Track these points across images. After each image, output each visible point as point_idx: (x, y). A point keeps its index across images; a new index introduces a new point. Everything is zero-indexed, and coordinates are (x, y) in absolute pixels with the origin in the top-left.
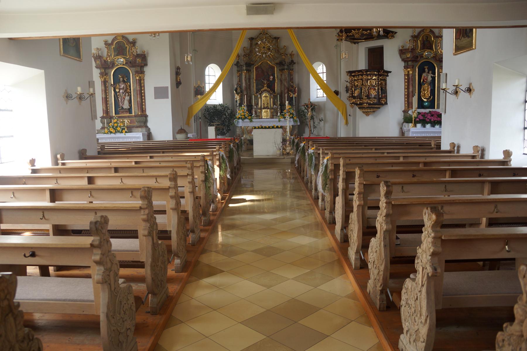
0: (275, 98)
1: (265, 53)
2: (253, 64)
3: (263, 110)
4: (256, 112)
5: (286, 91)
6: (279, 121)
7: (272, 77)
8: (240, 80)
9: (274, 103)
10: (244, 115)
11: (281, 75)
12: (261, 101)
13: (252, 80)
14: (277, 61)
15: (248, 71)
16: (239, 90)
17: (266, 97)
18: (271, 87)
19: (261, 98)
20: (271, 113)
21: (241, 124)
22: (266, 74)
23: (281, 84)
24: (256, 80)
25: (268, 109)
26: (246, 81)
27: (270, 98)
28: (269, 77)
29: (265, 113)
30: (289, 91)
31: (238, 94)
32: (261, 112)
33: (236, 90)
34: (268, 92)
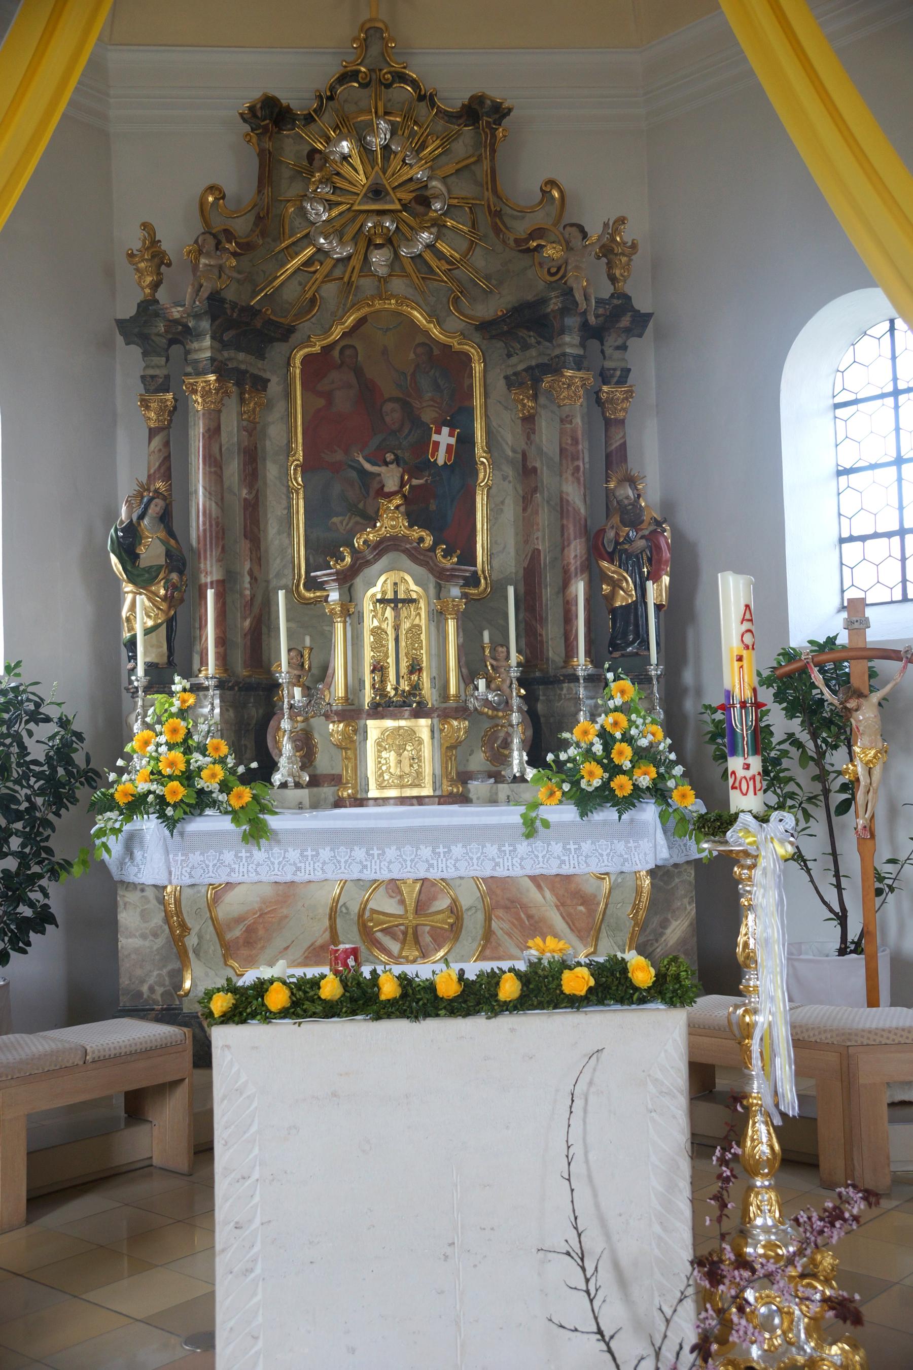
0: (478, 615)
1: (390, 241)
2: (286, 333)
3: (374, 728)
4: (306, 745)
5: (576, 550)
6: (531, 828)
7: (444, 438)
8: (169, 467)
9: (471, 670)
10: (188, 777)
11: (529, 420)
13: (272, 471)
14: (488, 310)
15: (244, 383)
16: (152, 550)
17: (396, 602)
18: (441, 512)
19: (350, 610)
20: (450, 750)
21: (155, 859)
22: (392, 414)
23: (526, 501)
24: (306, 468)
25: (420, 712)
26: (215, 464)
27: (438, 617)
28: (424, 444)
29: (394, 755)
30: (597, 549)
31: (141, 578)
32: (352, 746)
33: (128, 548)
34: (419, 556)
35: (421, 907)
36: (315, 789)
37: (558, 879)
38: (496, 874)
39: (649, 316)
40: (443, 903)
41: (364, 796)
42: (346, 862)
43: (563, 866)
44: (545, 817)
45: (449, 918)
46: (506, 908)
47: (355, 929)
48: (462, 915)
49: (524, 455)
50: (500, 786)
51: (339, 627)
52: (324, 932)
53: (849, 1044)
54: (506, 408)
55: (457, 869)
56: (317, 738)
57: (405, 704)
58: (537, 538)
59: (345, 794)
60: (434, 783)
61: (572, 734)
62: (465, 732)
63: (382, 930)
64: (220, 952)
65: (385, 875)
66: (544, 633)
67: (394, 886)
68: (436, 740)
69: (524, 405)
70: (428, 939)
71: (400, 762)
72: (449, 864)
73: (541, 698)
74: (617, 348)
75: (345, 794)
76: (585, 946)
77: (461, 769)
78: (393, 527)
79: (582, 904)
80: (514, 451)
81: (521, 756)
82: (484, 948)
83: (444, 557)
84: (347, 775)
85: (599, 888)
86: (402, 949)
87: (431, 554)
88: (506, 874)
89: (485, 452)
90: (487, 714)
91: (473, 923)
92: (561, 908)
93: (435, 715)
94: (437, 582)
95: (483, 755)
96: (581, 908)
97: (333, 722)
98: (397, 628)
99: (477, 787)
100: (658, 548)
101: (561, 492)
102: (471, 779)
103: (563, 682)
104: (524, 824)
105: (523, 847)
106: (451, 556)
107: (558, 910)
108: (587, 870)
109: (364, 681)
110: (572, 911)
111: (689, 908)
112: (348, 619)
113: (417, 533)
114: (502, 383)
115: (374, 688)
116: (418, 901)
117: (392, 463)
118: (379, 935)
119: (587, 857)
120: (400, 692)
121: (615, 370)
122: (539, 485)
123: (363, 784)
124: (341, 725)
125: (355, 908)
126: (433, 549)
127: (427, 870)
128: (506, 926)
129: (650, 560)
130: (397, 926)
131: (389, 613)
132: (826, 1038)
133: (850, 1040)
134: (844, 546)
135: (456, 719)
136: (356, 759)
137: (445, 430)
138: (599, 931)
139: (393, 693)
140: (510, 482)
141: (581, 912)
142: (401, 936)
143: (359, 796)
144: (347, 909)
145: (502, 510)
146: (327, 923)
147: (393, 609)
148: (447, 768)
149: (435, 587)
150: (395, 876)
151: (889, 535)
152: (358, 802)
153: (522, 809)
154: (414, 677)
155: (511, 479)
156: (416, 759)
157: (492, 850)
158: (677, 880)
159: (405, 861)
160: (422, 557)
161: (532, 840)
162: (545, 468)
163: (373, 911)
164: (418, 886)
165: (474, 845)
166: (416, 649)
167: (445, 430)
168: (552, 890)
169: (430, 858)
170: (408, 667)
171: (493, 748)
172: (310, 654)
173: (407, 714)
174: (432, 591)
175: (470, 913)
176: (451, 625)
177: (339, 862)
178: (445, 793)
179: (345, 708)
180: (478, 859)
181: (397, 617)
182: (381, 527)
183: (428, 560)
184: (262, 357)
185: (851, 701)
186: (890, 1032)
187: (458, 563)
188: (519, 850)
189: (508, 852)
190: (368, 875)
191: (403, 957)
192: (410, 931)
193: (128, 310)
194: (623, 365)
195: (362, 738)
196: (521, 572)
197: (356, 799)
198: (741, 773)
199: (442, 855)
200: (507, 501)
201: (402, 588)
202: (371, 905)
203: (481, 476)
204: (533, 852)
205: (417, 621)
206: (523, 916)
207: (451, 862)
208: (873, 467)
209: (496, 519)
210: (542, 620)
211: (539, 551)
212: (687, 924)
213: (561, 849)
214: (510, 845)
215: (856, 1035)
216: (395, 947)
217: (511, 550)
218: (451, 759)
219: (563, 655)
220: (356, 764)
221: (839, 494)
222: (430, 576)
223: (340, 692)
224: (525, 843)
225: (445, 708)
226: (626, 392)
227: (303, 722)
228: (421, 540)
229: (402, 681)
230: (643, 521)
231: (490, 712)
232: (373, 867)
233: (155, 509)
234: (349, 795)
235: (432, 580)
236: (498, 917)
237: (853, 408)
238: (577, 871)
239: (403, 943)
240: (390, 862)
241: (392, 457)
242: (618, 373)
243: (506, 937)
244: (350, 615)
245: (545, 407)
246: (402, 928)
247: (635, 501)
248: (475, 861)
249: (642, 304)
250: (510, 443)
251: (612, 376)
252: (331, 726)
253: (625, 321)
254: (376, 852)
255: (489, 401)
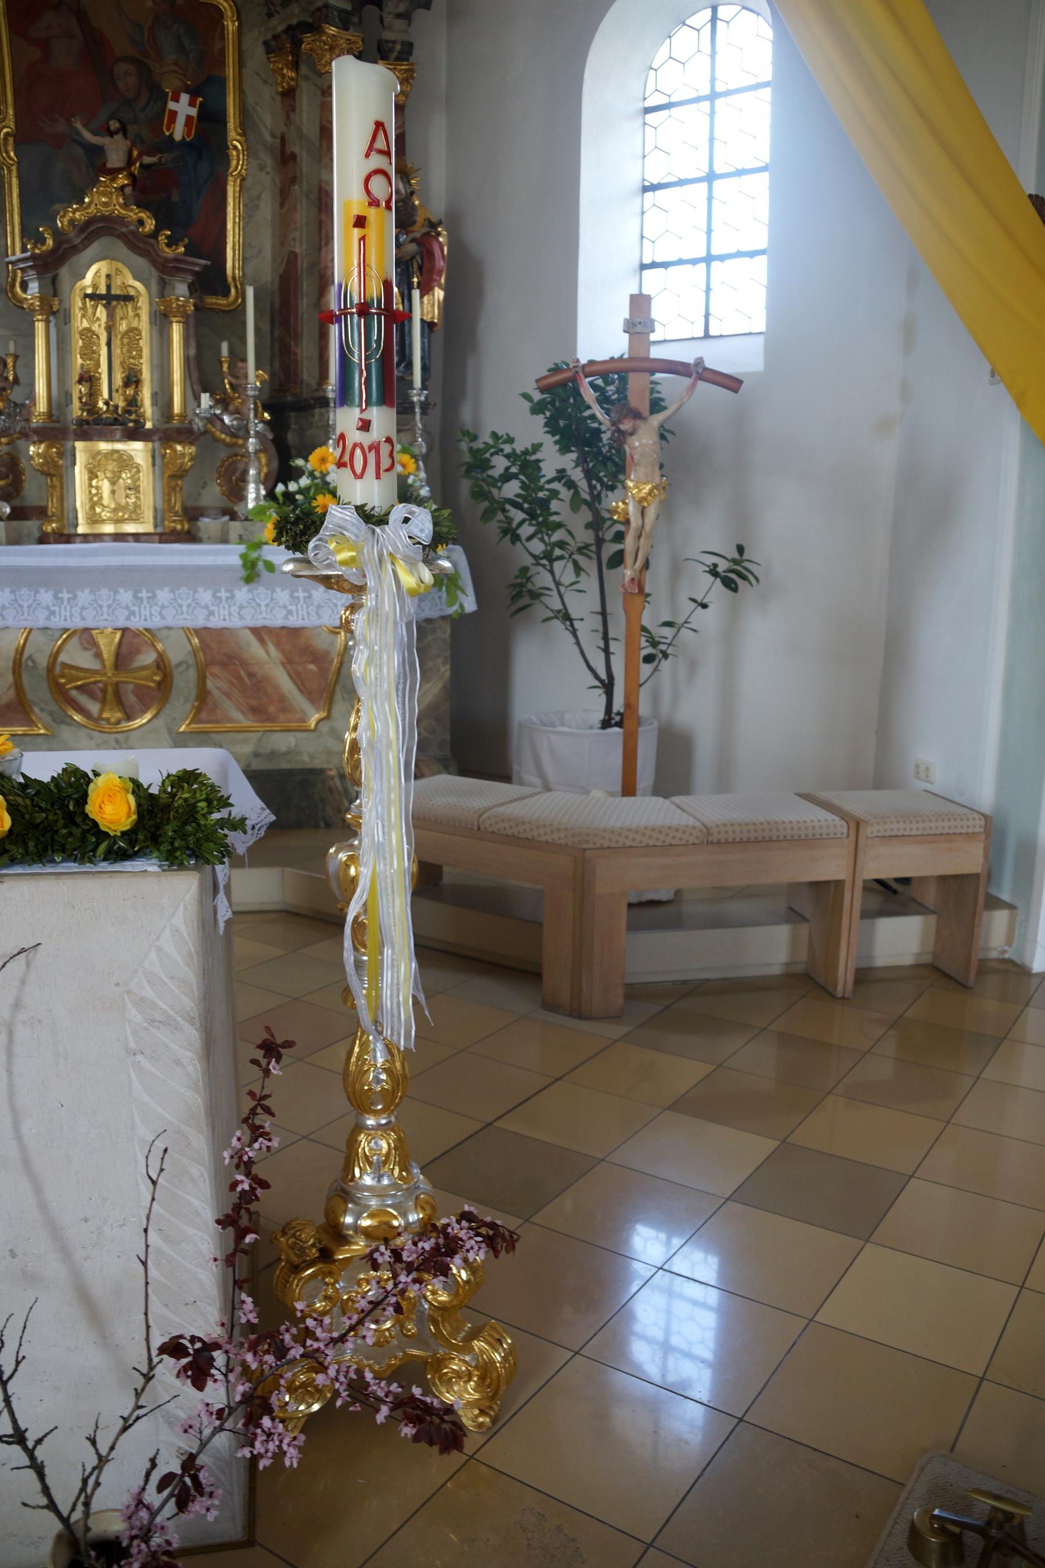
6: (252, 571)
7: (183, 108)
11: (289, 95)
12: (61, 347)
19: (54, 309)
20: (172, 477)
23: (284, 194)
27: (161, 320)
28: (163, 117)
29: (111, 484)
32: (57, 473)
34: (138, 244)
35: (122, 659)
36: (15, 523)
37: (284, 632)
38: (210, 625)
40: (148, 658)
41: (72, 531)
42: (29, 607)
43: (290, 617)
44: (269, 558)
45: (155, 674)
46: (223, 665)
47: (44, 686)
48: (171, 671)
49: (283, 139)
50: (233, 524)
51: (40, 327)
52: (8, 690)
53: (585, 846)
54: (265, 82)
55: (163, 617)
56: (23, 464)
57: (116, 422)
58: (294, 239)
59: (49, 529)
60: (155, 518)
61: (307, 461)
62: (191, 460)
63: (77, 688)
65: (77, 623)
66: (298, 351)
67: (86, 637)
68: (157, 468)
69: (283, 76)
70: (132, 699)
71: (113, 492)
72: (153, 612)
73: (293, 426)
74: (399, 16)
75: (49, 529)
76: (318, 710)
77: (191, 503)
78: (106, 204)
79: (312, 662)
80: (273, 136)
81: (258, 491)
82: (199, 710)
83: (168, 245)
84: (52, 508)
85: (333, 643)
86: (102, 710)
87: (152, 241)
88: (222, 624)
89: (238, 134)
90: (223, 441)
91: (185, 682)
92: (288, 666)
93: (156, 437)
94: (161, 278)
95: (218, 488)
96: (312, 667)
97: (34, 443)
98: (109, 329)
99: (206, 523)
100: (431, 254)
101: (320, 181)
102: (202, 515)
103: (313, 407)
104: (244, 566)
105: (242, 593)
106: (177, 245)
107: (285, 668)
108: (318, 622)
109: (71, 395)
110: (301, 669)
111: (442, 669)
112: (51, 318)
113: (134, 214)
114: (260, 49)
115: (81, 402)
116: (118, 655)
117: (117, 132)
118: (74, 693)
119: (319, 607)
120: (111, 408)
121: (394, 42)
122: (298, 174)
123: (71, 516)
124: (43, 446)
125: (43, 662)
126: (155, 235)
127: (128, 619)
128: (224, 685)
129: (420, 268)
130: (95, 683)
131: (101, 312)
132: (559, 838)
133: (587, 842)
134: (645, 273)
135: (179, 443)
136: (62, 488)
137: (185, 98)
138: (332, 693)
139: (105, 408)
140: (268, 173)
141: (311, 670)
142: (100, 695)
143: (66, 532)
144: (34, 662)
145: (257, 206)
146: (10, 678)
147: (104, 306)
148: (169, 501)
149: (159, 283)
150: (89, 623)
151: (694, 262)
152: (64, 538)
153: (242, 548)
154: (130, 392)
155: (269, 169)
156: (135, 488)
157: (205, 596)
158: (430, 638)
159: (101, 606)
160: (141, 245)
161: (253, 585)
162: (304, 153)
163: (64, 665)
164: (118, 635)
165: (184, 590)
166: (134, 358)
167: (185, 98)
168: (278, 645)
169: (130, 604)
170: (123, 378)
171: (230, 481)
172: (15, 363)
173: (118, 434)
174: (154, 288)
175: (180, 669)
176: (177, 331)
177: (21, 607)
178: (167, 531)
179: (48, 425)
180: (189, 606)
181: (111, 316)
182: (90, 203)
183: (149, 248)
185: (626, 421)
186: (637, 832)
187: (186, 254)
188: (237, 597)
189: (224, 599)
190: (57, 622)
191: (104, 719)
192: (110, 689)
194: (404, 37)
195: (69, 463)
196: (277, 282)
197: (61, 535)
198: (354, 436)
199: (145, 601)
200: (263, 196)
201: (117, 281)
202: (63, 658)
203: (234, 163)
204: (253, 599)
205: (135, 324)
206: (243, 673)
207: (156, 609)
208: (681, 183)
209: (250, 216)
210: (297, 337)
211: (295, 255)
212: (439, 686)
213: (287, 597)
214: (227, 591)
215: (595, 836)
216: (94, 708)
217: (268, 255)
218: (174, 490)
219: (317, 377)
220: (62, 494)
221: (643, 213)
222: (153, 269)
223: (42, 406)
224: (245, 589)
225: (166, 430)
226: (406, 71)
227: (8, 444)
228: (141, 222)
229: (114, 394)
230: (414, 223)
231: (228, 439)
232: (63, 613)
234: (53, 529)
235: (155, 273)
236: (214, 676)
237: (664, 113)
238: (306, 623)
239: (103, 702)
240: (83, 608)
241: (117, 125)
242: (398, 47)
243: (224, 698)
244: (54, 313)
245: (306, 78)
246: (100, 685)
247: (407, 197)
248: (185, 608)
250: (269, 126)
251: (391, 50)
252: (32, 448)
254: (65, 595)
255: (244, 72)
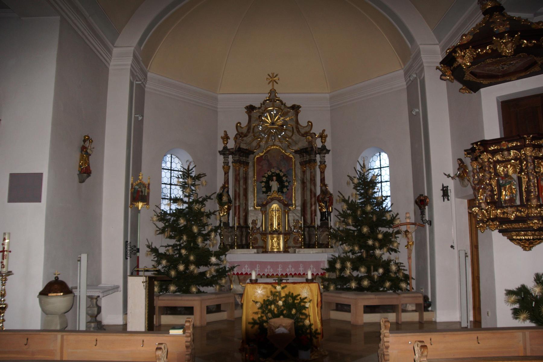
14: (296, 148)
39: (329, 150)
64: (238, 281)
114: (299, 164)
184: (248, 157)
193: (221, 148)
233: (226, 190)
249: (328, 148)
253: (324, 152)
